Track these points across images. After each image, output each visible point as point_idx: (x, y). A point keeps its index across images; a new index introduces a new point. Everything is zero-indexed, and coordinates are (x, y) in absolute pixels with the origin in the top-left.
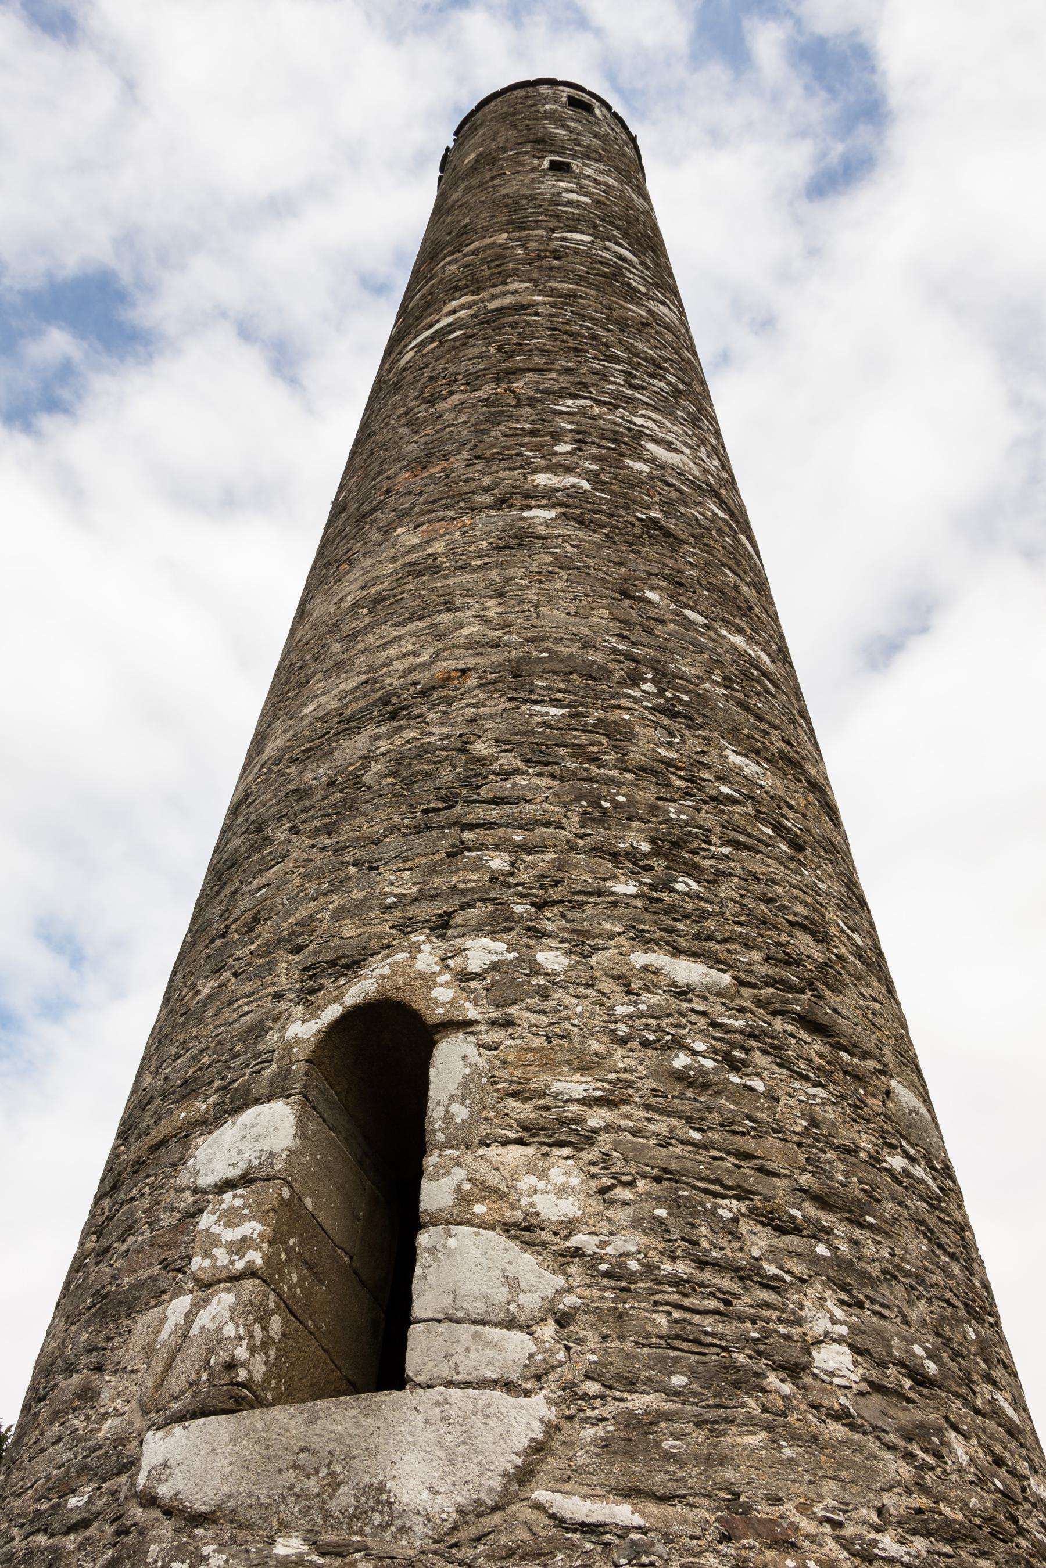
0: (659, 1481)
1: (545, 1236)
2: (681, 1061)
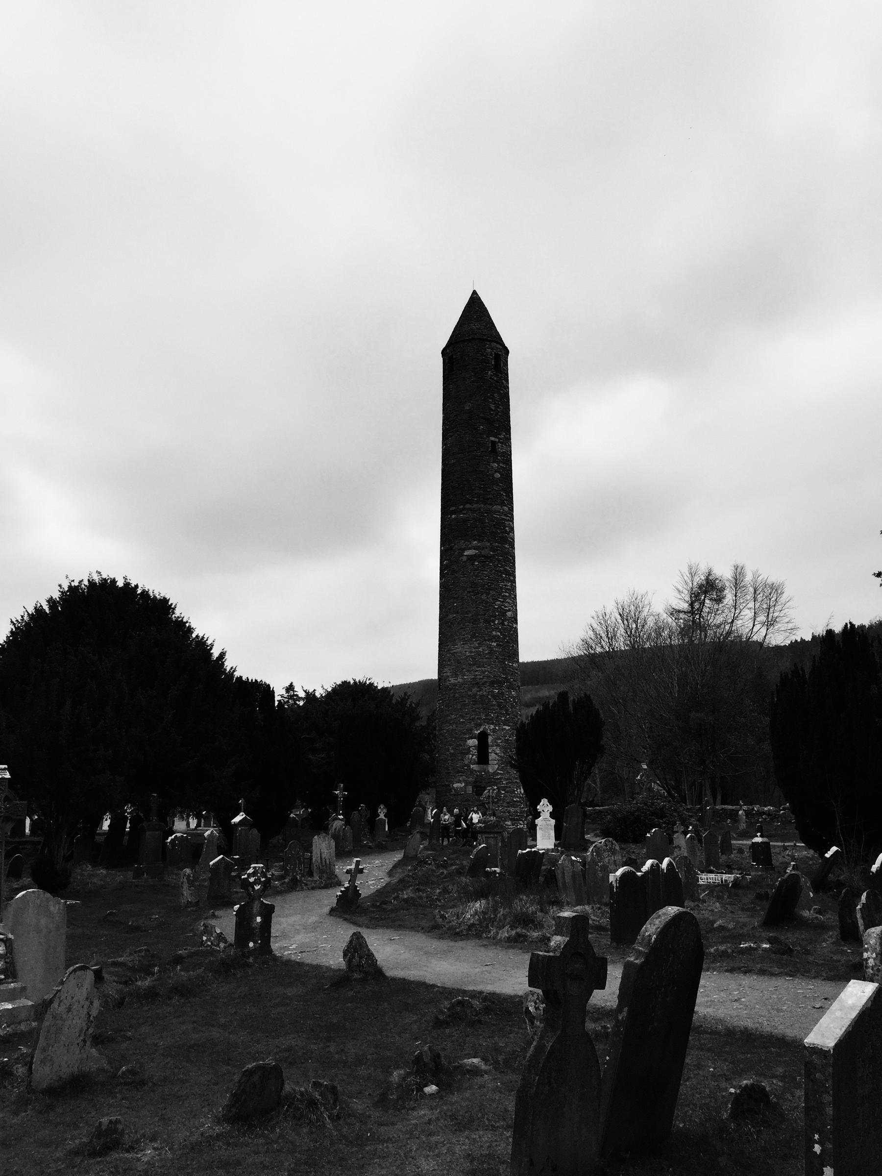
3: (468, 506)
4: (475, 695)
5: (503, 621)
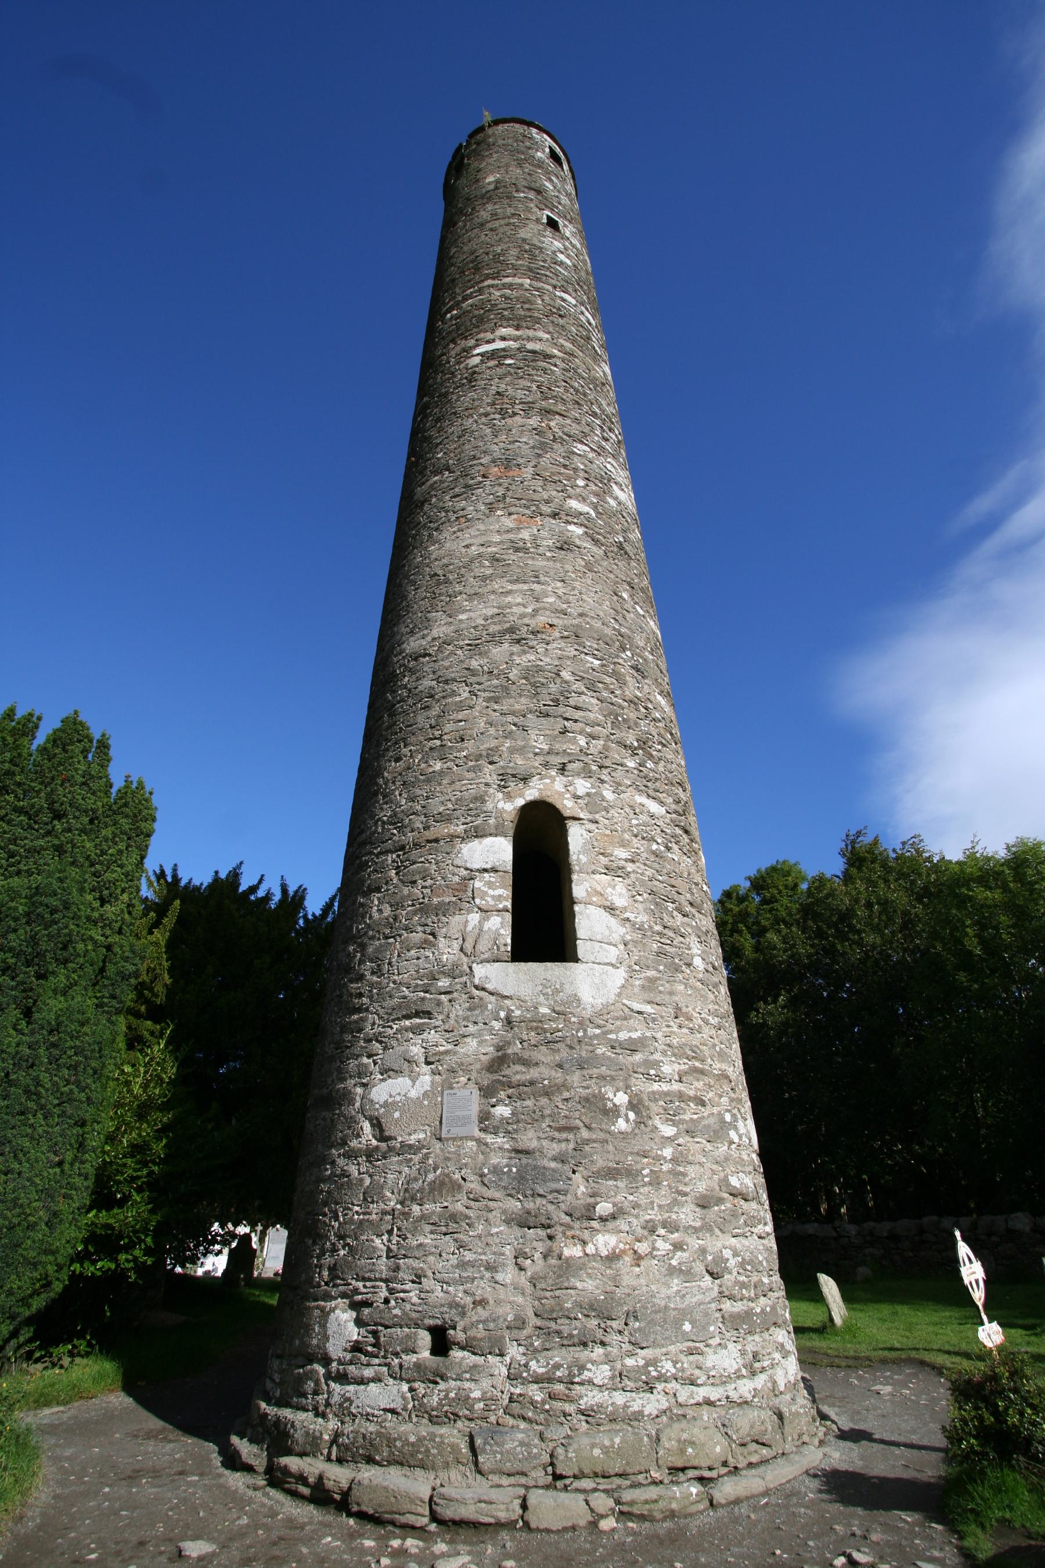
0: (658, 1000)
1: (618, 912)
2: (654, 847)
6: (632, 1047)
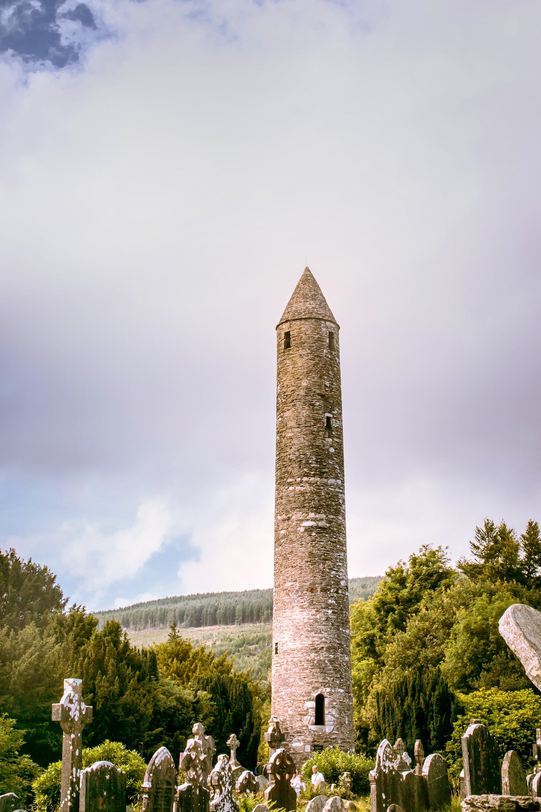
3: (305, 479)
4: (314, 660)
5: (338, 590)
6: (334, 739)
